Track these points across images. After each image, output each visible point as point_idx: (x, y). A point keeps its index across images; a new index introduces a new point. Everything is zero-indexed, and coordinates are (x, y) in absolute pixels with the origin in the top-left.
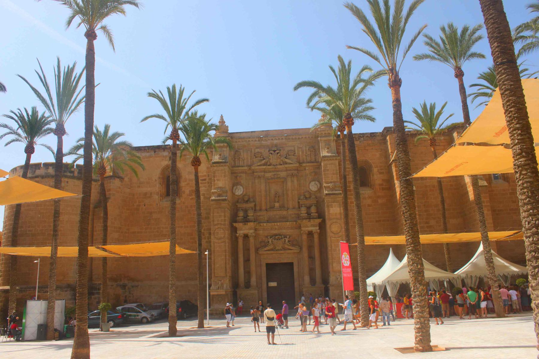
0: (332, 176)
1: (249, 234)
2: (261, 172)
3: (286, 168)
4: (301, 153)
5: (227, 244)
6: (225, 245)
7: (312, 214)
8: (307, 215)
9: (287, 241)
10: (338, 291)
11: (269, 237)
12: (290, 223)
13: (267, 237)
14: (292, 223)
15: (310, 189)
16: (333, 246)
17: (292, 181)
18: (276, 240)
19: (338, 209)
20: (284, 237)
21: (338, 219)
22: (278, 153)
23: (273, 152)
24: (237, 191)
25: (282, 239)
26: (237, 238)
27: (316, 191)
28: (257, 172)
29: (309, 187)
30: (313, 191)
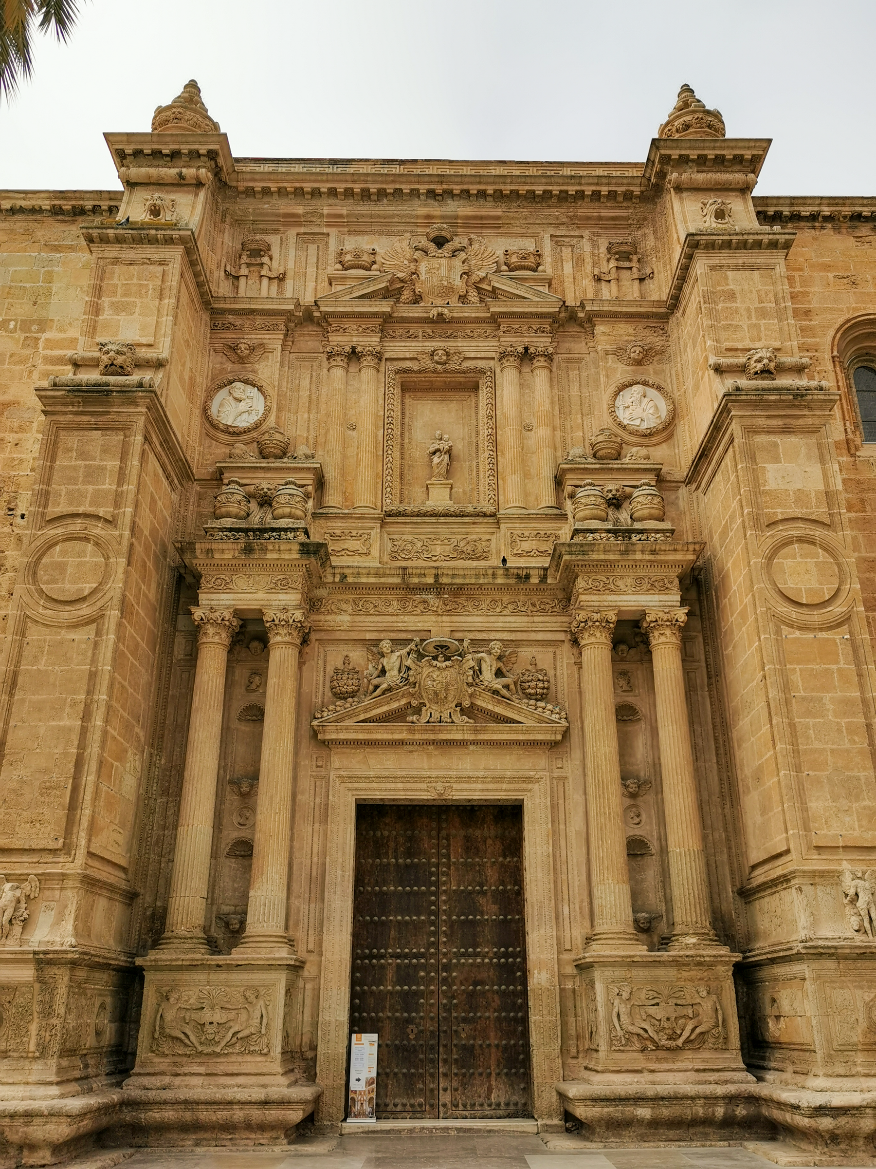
0: (757, 326)
1: (269, 615)
4: (568, 268)
5: (112, 637)
6: (96, 645)
15: (615, 418)
16: (796, 678)
19: (816, 470)
22: (454, 253)
23: (432, 246)
26: (195, 633)
27: (648, 435)
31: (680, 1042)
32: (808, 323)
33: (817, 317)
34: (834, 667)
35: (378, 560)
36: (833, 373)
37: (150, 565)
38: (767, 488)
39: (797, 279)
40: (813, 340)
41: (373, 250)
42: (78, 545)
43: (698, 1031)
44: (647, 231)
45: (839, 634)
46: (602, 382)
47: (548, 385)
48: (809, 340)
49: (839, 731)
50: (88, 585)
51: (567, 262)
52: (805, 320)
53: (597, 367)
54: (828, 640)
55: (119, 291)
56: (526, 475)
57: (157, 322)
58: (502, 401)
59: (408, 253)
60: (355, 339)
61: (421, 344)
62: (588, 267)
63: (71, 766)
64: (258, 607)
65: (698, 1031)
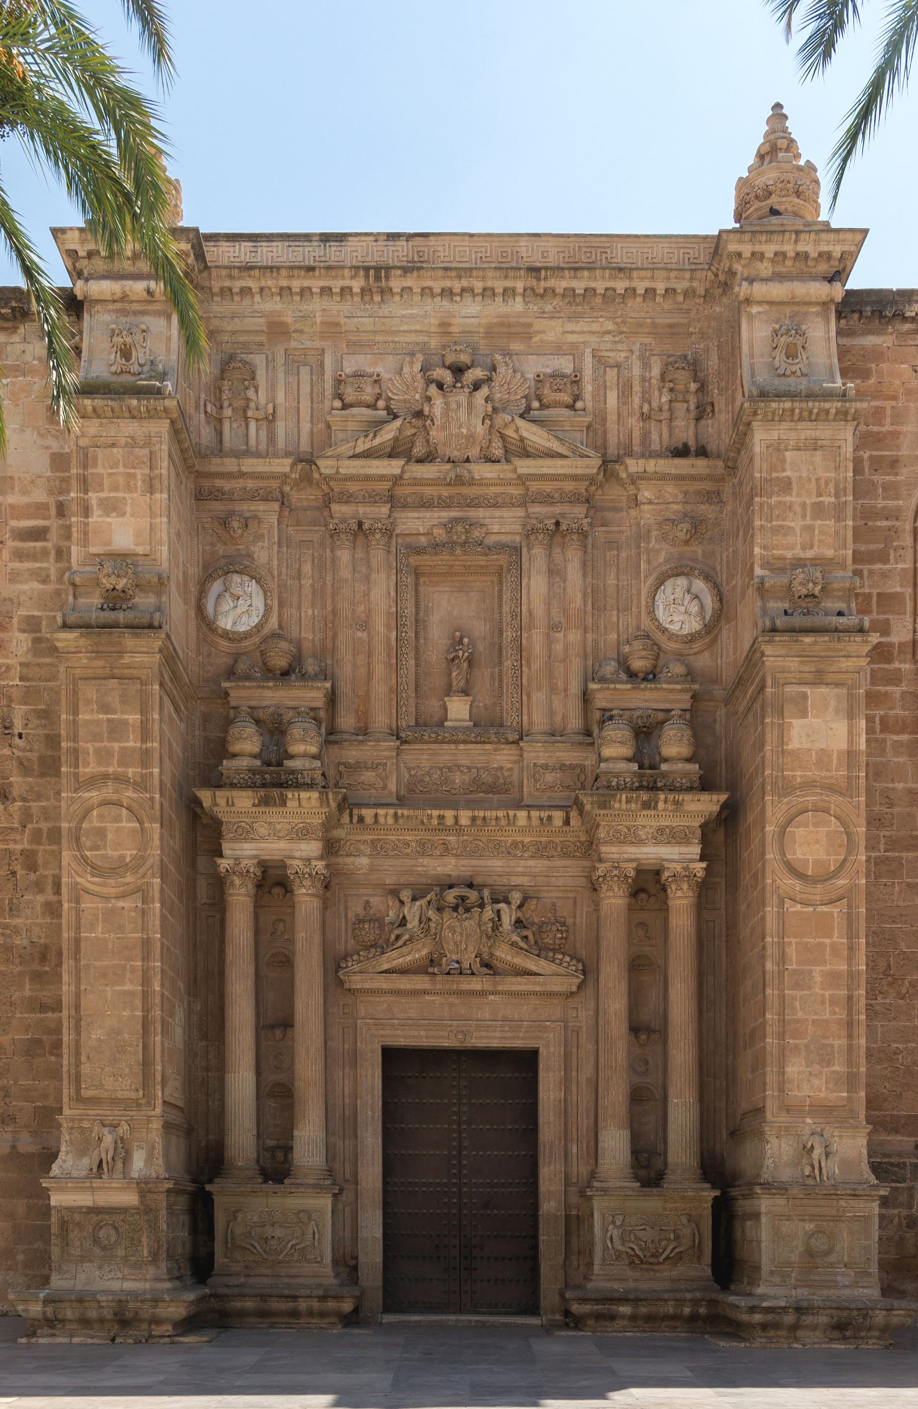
2: (373, 498)
3: (523, 480)
7: (664, 767)
8: (635, 767)
9: (508, 918)
10: (809, 1226)
11: (405, 895)
12: (535, 814)
13: (394, 892)
14: (544, 814)
15: (654, 619)
16: (792, 952)
17: (554, 572)
18: (447, 914)
20: (496, 901)
21: (832, 789)
24: (227, 604)
25: (482, 906)
26: (219, 883)
27: (691, 639)
28: (347, 498)
29: (652, 612)
30: (672, 637)
31: (661, 1259)
32: (892, 478)
33: (904, 470)
34: (827, 941)
35: (395, 796)
36: (911, 551)
37: (173, 816)
38: (790, 747)
39: (888, 412)
40: (895, 503)
42: (114, 810)
43: (677, 1250)
44: (711, 345)
45: (836, 907)
46: (642, 570)
47: (580, 574)
48: (891, 503)
49: (823, 1003)
50: (129, 853)
51: (612, 390)
52: (889, 474)
53: (639, 547)
54: (825, 913)
55: (106, 483)
56: (553, 689)
57: (151, 524)
58: (529, 593)
59: (420, 384)
60: (361, 510)
61: (436, 515)
62: (637, 400)
63: (140, 1027)
64: (281, 858)
65: (677, 1250)
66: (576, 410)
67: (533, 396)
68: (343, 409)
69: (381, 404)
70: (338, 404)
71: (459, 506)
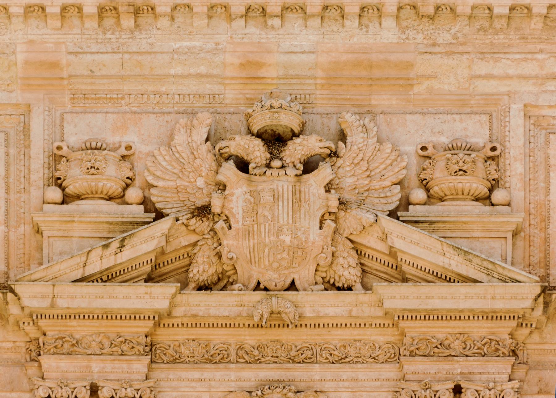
41: (128, 148)
61: (233, 376)
66: (493, 205)
67: (415, 182)
68: (63, 203)
69: (133, 194)
70: (55, 194)
71: (276, 360)
